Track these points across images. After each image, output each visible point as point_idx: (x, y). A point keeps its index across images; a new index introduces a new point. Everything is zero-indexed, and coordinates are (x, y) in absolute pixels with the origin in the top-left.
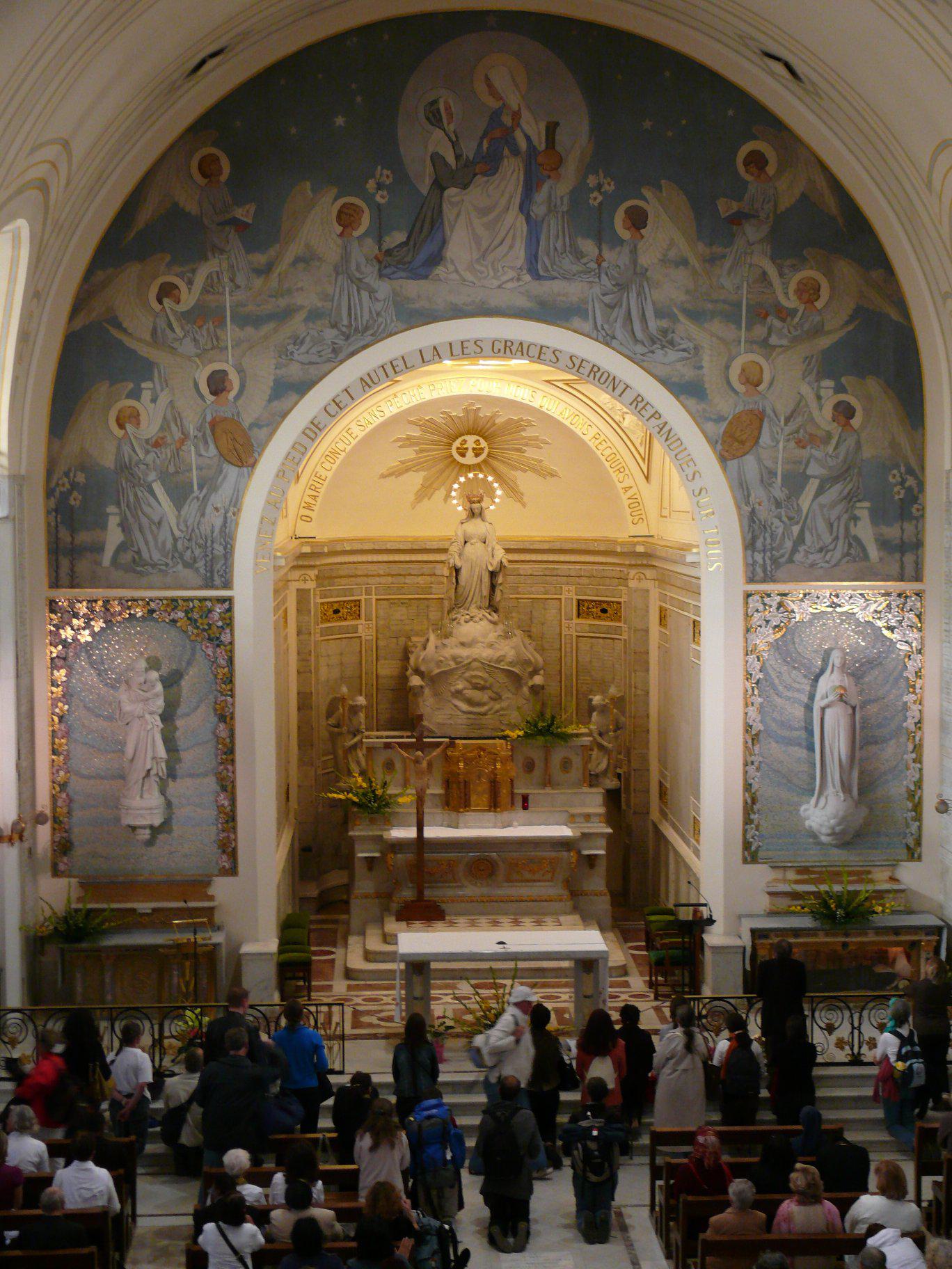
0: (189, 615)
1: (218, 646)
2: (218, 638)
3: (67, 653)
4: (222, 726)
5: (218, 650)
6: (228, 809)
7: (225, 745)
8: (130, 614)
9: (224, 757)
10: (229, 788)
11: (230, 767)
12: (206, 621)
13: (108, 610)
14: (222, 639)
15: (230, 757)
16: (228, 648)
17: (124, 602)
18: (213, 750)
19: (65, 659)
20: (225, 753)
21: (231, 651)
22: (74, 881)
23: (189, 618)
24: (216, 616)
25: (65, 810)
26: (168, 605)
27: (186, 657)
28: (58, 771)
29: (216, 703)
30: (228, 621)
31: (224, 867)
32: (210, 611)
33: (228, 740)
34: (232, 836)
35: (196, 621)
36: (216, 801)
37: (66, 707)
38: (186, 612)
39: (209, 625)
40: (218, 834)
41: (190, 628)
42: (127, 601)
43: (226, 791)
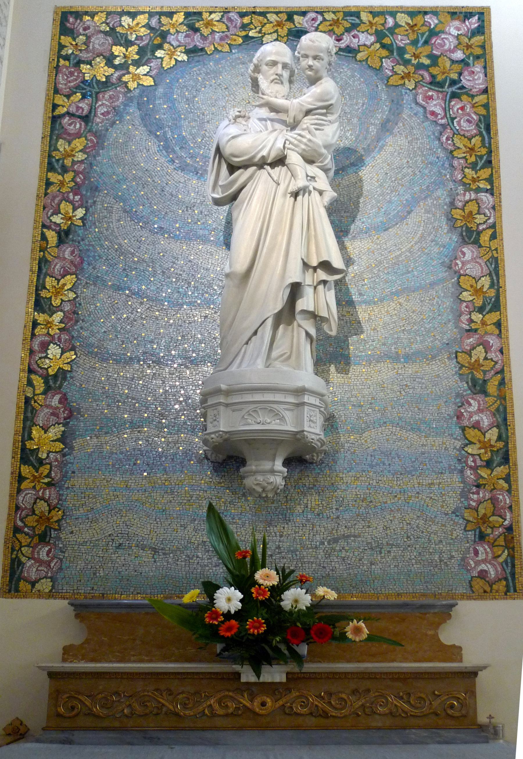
0: (386, 41)
1: (454, 96)
2: (453, 83)
3: (92, 109)
4: (469, 252)
5: (456, 105)
6: (492, 435)
7: (477, 291)
8: (247, 38)
9: (477, 317)
10: (492, 388)
11: (492, 340)
12: (426, 50)
13: (196, 30)
14: (465, 81)
15: (494, 317)
16: (482, 99)
17: (233, 16)
18: (448, 302)
19: (86, 119)
20: (481, 310)
21: (486, 106)
22: (61, 604)
23: (383, 46)
24: (450, 42)
25: (55, 432)
26: (336, 22)
27: (379, 117)
28: (45, 346)
29: (452, 205)
30: (478, 51)
31: (483, 574)
32: (433, 33)
33: (485, 282)
34: (504, 499)
35: (402, 51)
36: (459, 416)
37: (80, 213)
38: (380, 36)
39: (431, 56)
40: (464, 495)
41: (387, 64)
42: (242, 15)
43: (484, 392)
